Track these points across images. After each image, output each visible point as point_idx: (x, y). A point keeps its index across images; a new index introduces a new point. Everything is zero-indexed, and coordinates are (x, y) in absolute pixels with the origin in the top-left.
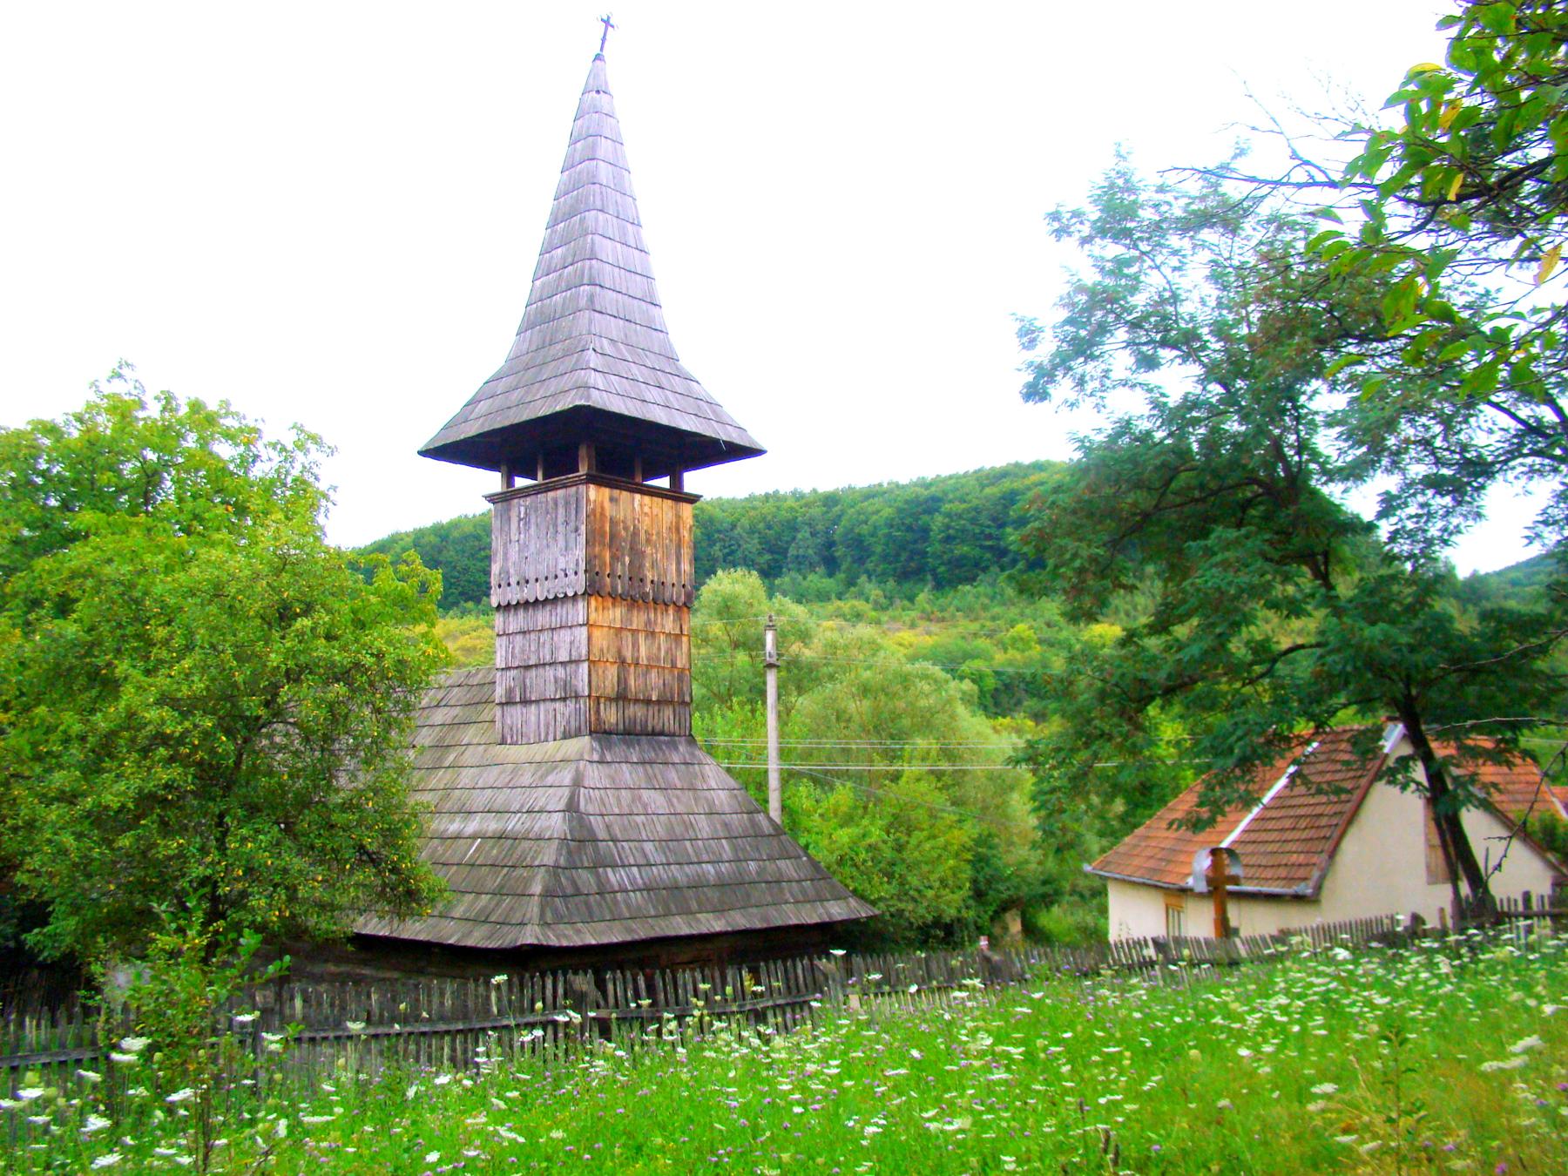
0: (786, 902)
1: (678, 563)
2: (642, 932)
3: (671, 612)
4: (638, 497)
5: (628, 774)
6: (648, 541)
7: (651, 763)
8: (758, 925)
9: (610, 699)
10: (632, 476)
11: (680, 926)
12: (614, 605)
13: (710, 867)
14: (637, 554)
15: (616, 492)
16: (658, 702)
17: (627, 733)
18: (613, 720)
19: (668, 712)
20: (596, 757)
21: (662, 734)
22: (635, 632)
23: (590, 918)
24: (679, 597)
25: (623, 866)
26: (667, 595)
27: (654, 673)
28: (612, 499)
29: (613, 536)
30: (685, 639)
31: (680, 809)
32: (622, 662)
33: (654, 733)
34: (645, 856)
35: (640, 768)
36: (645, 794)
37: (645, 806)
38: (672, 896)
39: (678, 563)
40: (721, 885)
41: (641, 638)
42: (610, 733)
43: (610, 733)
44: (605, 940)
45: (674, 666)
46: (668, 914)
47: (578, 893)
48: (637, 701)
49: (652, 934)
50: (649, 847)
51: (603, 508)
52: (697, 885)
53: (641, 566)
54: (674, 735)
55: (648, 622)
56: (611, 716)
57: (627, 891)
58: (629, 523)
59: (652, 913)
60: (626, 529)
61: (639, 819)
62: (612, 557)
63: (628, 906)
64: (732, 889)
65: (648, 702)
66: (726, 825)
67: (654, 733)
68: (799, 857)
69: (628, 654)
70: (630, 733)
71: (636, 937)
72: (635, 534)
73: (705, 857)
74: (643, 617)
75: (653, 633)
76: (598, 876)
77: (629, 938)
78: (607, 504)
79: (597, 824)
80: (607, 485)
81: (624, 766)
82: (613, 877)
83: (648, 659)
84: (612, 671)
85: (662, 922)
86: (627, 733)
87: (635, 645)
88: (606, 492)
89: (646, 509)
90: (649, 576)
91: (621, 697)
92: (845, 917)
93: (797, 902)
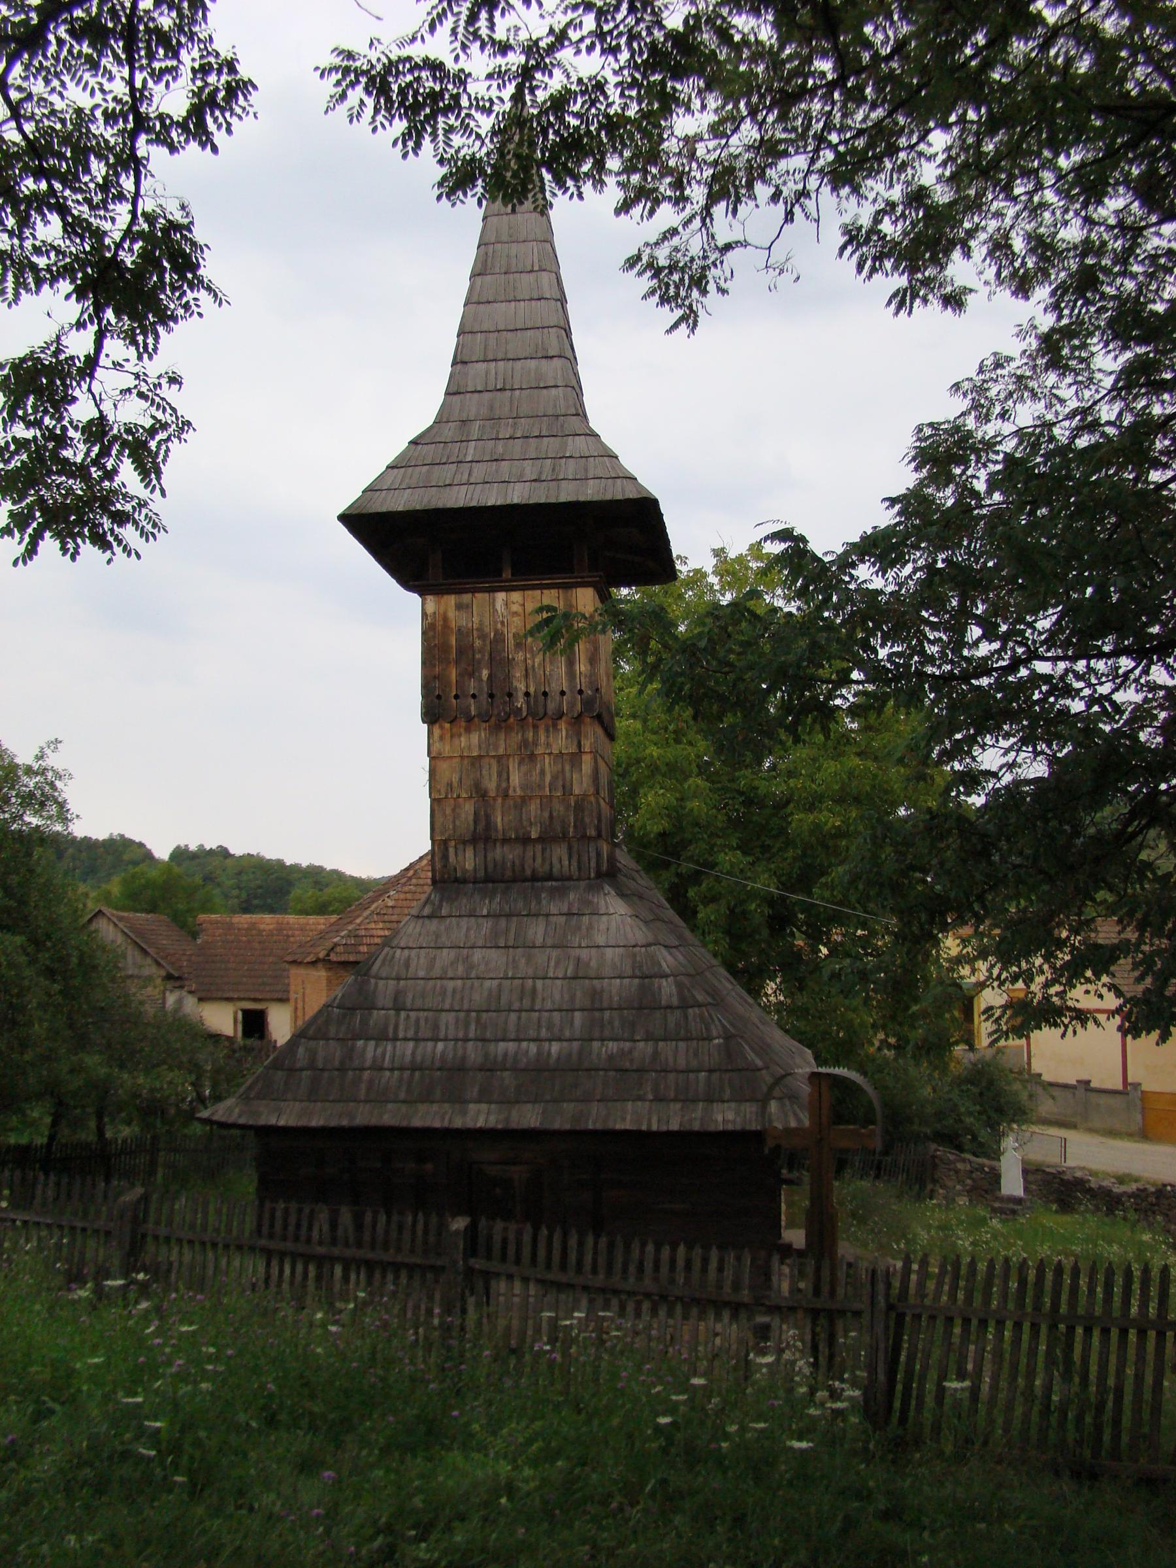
0: (640, 1098)
1: (571, 663)
2: (364, 1116)
3: (562, 725)
4: (501, 596)
5: (460, 930)
6: (519, 646)
7: (509, 916)
8: (557, 1125)
9: (465, 843)
10: (498, 572)
11: (429, 1116)
12: (468, 730)
13: (533, 1048)
14: (499, 662)
15: (466, 598)
16: (540, 839)
17: (488, 879)
18: (469, 865)
19: (559, 853)
20: (427, 911)
21: (550, 877)
22: (499, 758)
23: (313, 1095)
24: (572, 705)
25: (396, 1039)
26: (551, 706)
27: (533, 807)
28: (459, 607)
29: (461, 651)
30: (587, 759)
31: (523, 968)
32: (480, 794)
33: (535, 878)
34: (436, 1027)
35: (487, 925)
36: (477, 955)
37: (471, 967)
38: (451, 1080)
39: (571, 663)
40: (540, 1070)
41: (513, 765)
42: (464, 881)
43: (464, 881)
44: (303, 1122)
45: (567, 790)
46: (426, 1098)
47: (312, 1066)
48: (506, 841)
49: (374, 1121)
50: (447, 1018)
51: (445, 619)
52: (489, 1068)
53: (508, 677)
54: (570, 878)
55: (525, 743)
56: (468, 861)
57: (381, 1069)
58: (487, 630)
59: (402, 1096)
60: (483, 637)
61: (450, 985)
62: (460, 675)
63: (369, 1089)
64: (539, 1077)
65: (525, 840)
66: (595, 994)
67: (535, 878)
68: (709, 1039)
69: (491, 785)
70: (492, 880)
71: (345, 1122)
72: (499, 638)
73: (532, 1033)
74: (516, 738)
75: (532, 757)
76: (353, 1049)
77: (334, 1123)
78: (452, 614)
79: (385, 990)
80: (449, 592)
81: (464, 922)
82: (370, 1050)
83: (524, 787)
84: (468, 808)
85: (404, 1108)
86: (488, 879)
87: (504, 774)
88: (451, 600)
89: (515, 608)
90: (522, 687)
91: (482, 836)
92: (738, 1127)
93: (658, 1099)
